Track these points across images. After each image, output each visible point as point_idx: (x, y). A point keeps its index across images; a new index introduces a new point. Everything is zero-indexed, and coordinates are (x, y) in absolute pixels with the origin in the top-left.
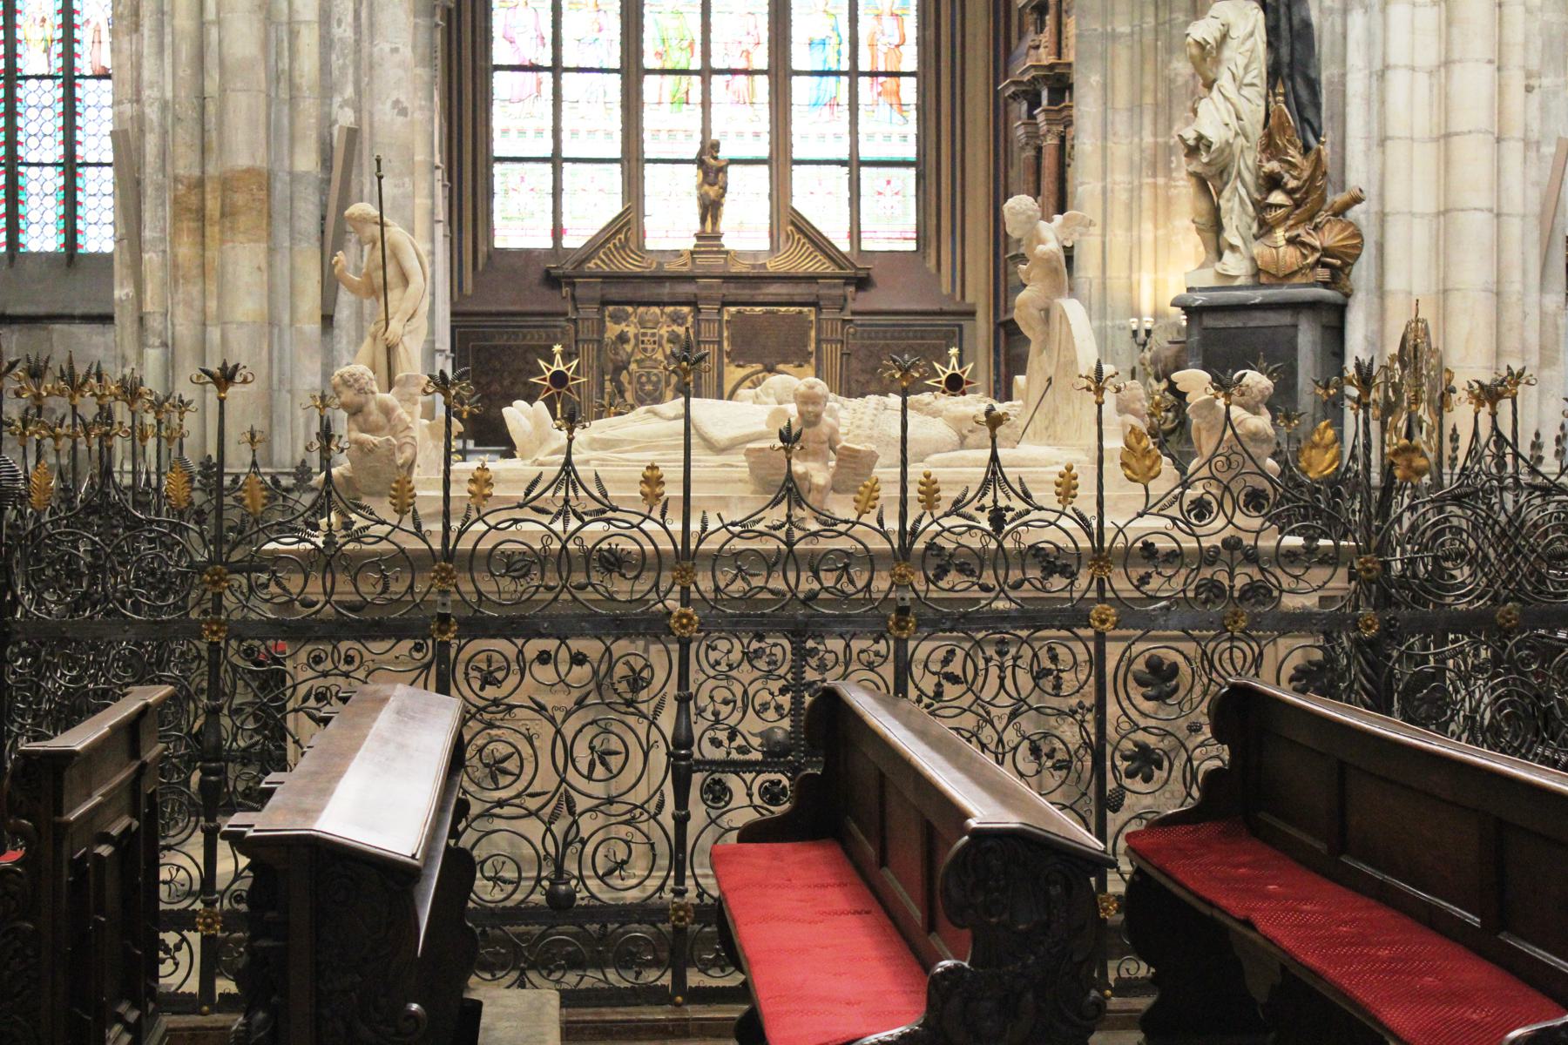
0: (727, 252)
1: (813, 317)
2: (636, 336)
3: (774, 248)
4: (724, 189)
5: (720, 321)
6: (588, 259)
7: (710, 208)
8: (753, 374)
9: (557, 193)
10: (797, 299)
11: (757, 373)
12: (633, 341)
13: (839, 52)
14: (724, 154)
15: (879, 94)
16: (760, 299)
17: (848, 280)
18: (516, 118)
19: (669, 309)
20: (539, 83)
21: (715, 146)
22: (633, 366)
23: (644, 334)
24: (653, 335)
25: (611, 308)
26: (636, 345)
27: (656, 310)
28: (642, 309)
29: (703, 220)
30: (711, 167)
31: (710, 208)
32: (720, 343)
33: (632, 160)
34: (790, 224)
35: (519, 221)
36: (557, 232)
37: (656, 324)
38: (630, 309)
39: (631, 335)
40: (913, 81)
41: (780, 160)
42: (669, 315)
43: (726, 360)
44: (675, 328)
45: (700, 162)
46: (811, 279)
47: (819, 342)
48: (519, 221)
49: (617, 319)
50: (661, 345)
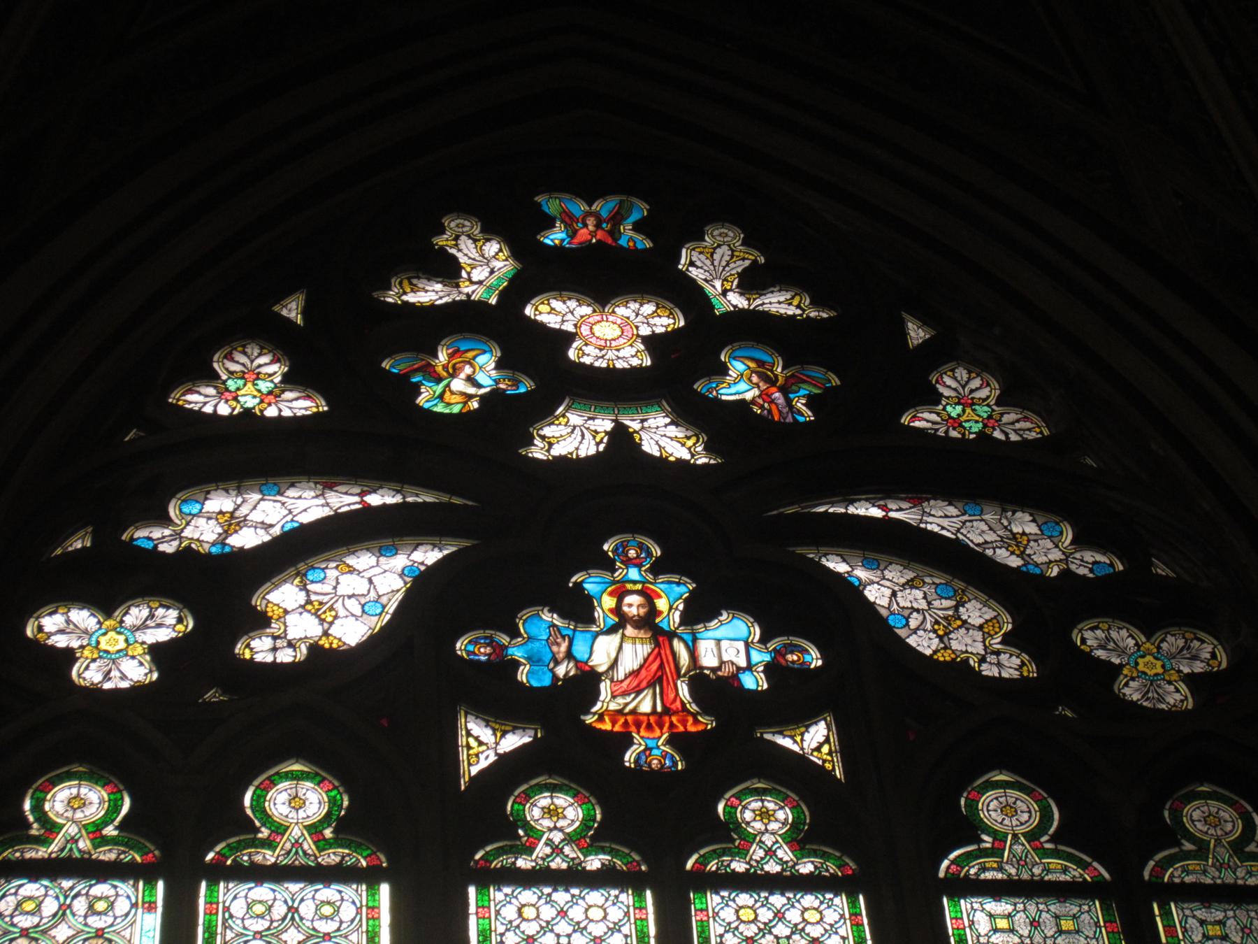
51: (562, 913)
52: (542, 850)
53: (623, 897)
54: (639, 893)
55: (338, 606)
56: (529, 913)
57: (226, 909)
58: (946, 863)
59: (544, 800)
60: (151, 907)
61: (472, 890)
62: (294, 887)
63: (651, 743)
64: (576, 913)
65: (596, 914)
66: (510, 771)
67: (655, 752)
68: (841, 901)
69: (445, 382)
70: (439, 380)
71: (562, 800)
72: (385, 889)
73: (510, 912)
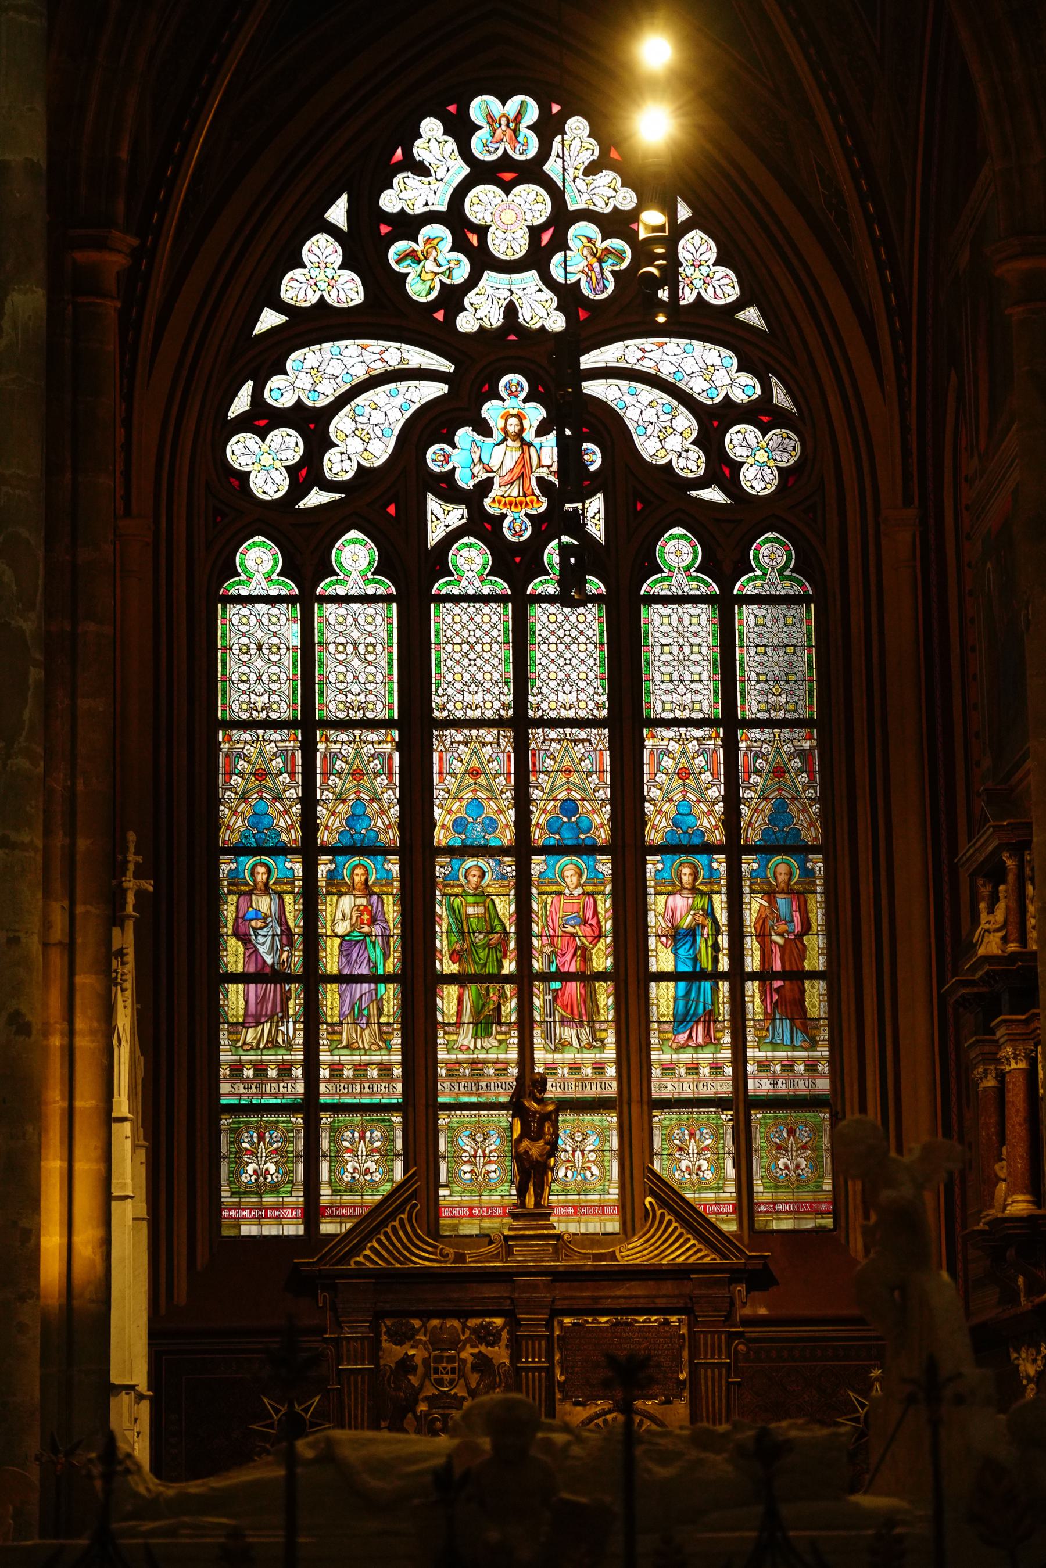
0: (558, 1237)
1: (684, 1331)
2: (426, 1361)
3: (628, 1230)
4: (553, 1148)
5: (550, 1339)
6: (357, 1250)
7: (532, 1172)
8: (598, 1416)
9: (311, 1156)
10: (661, 1303)
11: (604, 1413)
12: (421, 1370)
13: (716, 947)
14: (553, 1091)
15: (775, 1005)
16: (608, 1304)
17: (736, 1275)
18: (253, 1049)
19: (473, 1322)
20: (286, 998)
21: (541, 1083)
22: (423, 1407)
23: (439, 1359)
24: (451, 1359)
25: (388, 1322)
26: (426, 1375)
27: (456, 1323)
28: (435, 1322)
29: (522, 1193)
30: (534, 1112)
31: (532, 1172)
32: (550, 1371)
33: (420, 1107)
34: (646, 1192)
35: (261, 1197)
36: (312, 1212)
37: (456, 1344)
38: (417, 1323)
39: (418, 1360)
40: (821, 986)
41: (634, 1103)
42: (474, 1331)
43: (558, 1396)
44: (483, 1348)
45: (516, 1106)
46: (679, 1273)
47: (694, 1369)
48: (261, 1197)
49: (401, 1337)
50: (463, 1375)
51: (472, 619)
52: (464, 583)
53: (498, 609)
54: (506, 607)
55: (371, 432)
56: (457, 619)
57: (327, 620)
58: (645, 586)
59: (465, 552)
60: (295, 622)
61: (432, 605)
62: (355, 606)
63: (516, 516)
64: (478, 619)
65: (486, 619)
66: (453, 537)
67: (518, 521)
68: (595, 609)
69: (422, 264)
70: (419, 262)
71: (473, 552)
72: (395, 605)
73: (449, 619)
